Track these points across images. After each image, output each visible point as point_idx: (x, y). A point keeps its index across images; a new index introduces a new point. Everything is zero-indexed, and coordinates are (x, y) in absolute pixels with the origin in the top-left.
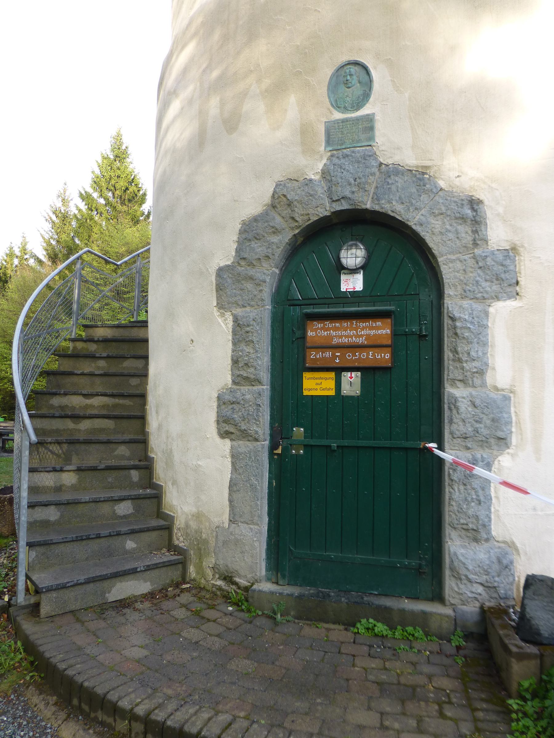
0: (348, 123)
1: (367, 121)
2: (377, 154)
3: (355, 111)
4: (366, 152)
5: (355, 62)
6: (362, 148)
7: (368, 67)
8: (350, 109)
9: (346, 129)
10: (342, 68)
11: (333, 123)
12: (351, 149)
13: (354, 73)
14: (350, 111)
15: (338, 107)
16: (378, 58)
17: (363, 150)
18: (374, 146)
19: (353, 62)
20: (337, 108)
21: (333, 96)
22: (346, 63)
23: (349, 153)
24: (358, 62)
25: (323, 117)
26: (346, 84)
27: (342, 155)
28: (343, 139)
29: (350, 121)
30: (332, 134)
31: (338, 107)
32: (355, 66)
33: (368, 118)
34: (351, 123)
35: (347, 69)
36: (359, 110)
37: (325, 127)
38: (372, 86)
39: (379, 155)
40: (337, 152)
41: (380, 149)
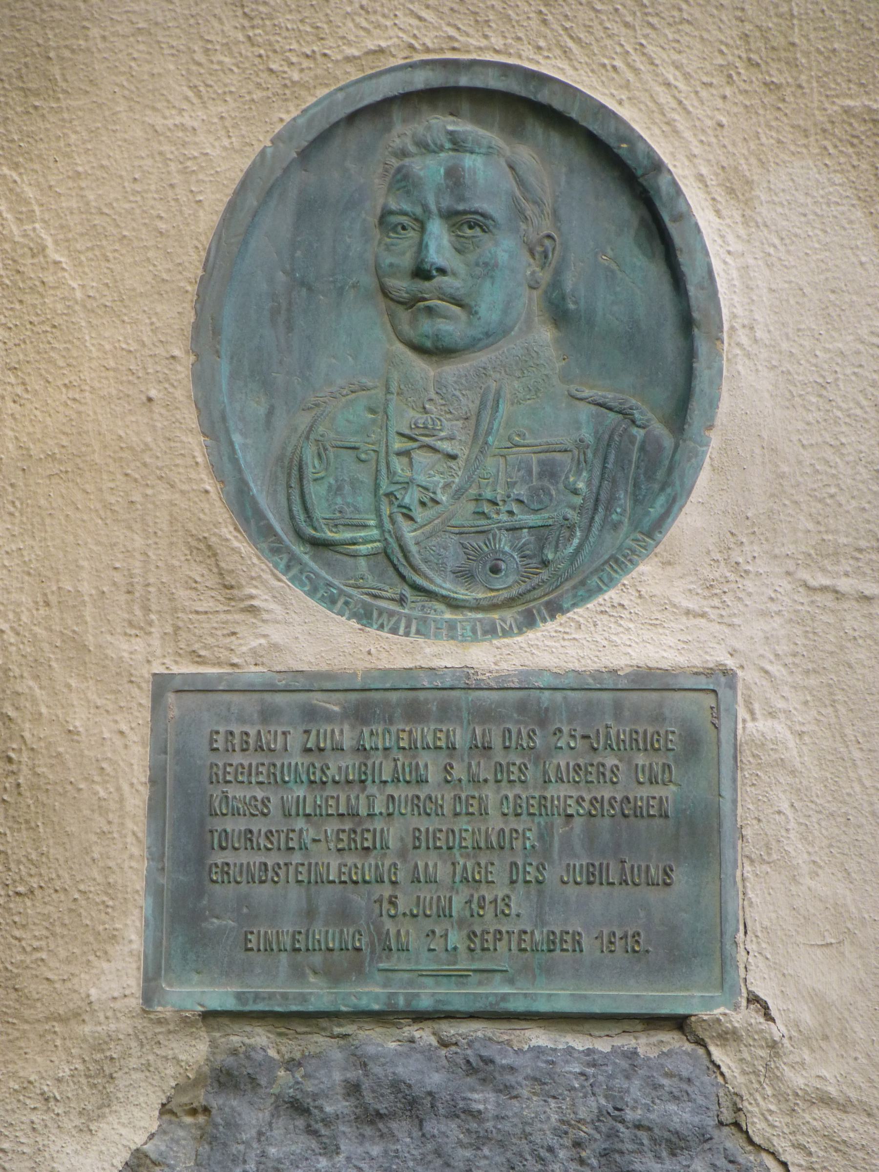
0: (425, 732)
1: (636, 743)
2: (757, 1128)
3: (510, 616)
4: (635, 1089)
5: (514, 86)
6: (579, 1042)
7: (658, 166)
8: (446, 586)
9: (401, 792)
10: (365, 130)
11: (249, 704)
12: (450, 1030)
13: (495, 208)
14: (454, 605)
15: (318, 545)
16: (771, 86)
17: (592, 1059)
18: (729, 1036)
19: (494, 82)
20: (299, 549)
21: (257, 408)
22: (420, 80)
23: (435, 1079)
24: (544, 96)
25: (144, 630)
26: (411, 303)
27: (353, 1089)
28: (359, 899)
29: (446, 712)
30: (234, 825)
31: (318, 545)
32: (515, 132)
33: (658, 718)
34: (460, 738)
35: (425, 147)
36: (554, 609)
37: (159, 747)
38: (701, 384)
39: (781, 1145)
40: (292, 1048)
41: (798, 1080)
